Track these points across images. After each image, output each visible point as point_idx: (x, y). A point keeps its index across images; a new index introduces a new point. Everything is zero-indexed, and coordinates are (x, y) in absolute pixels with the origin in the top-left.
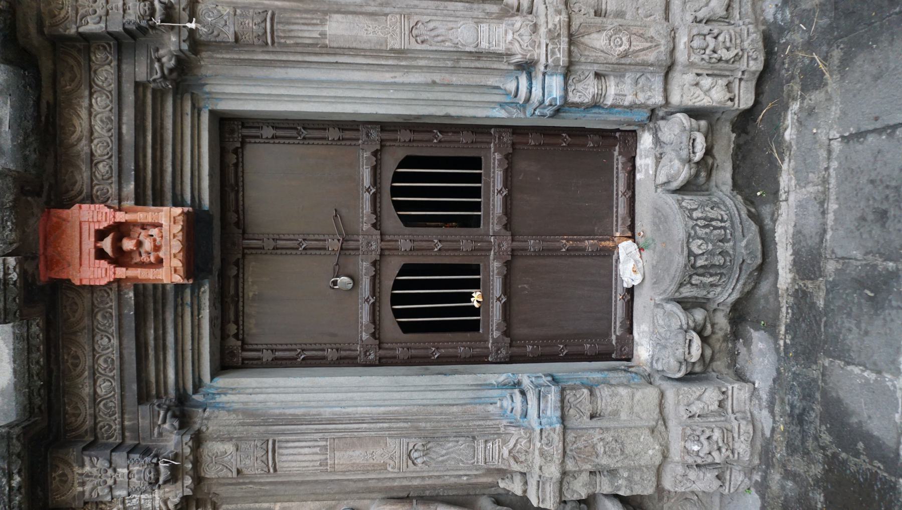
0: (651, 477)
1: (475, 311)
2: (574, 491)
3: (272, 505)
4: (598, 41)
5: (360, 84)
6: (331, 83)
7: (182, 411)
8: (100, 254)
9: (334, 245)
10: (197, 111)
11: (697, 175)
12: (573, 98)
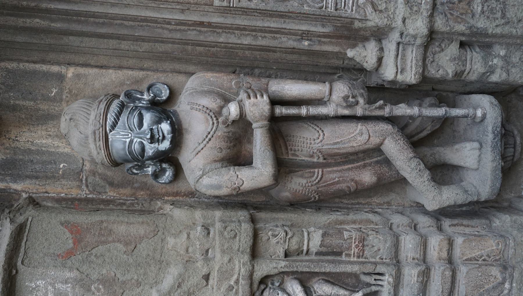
2: (439, 67)
3: (63, 69)
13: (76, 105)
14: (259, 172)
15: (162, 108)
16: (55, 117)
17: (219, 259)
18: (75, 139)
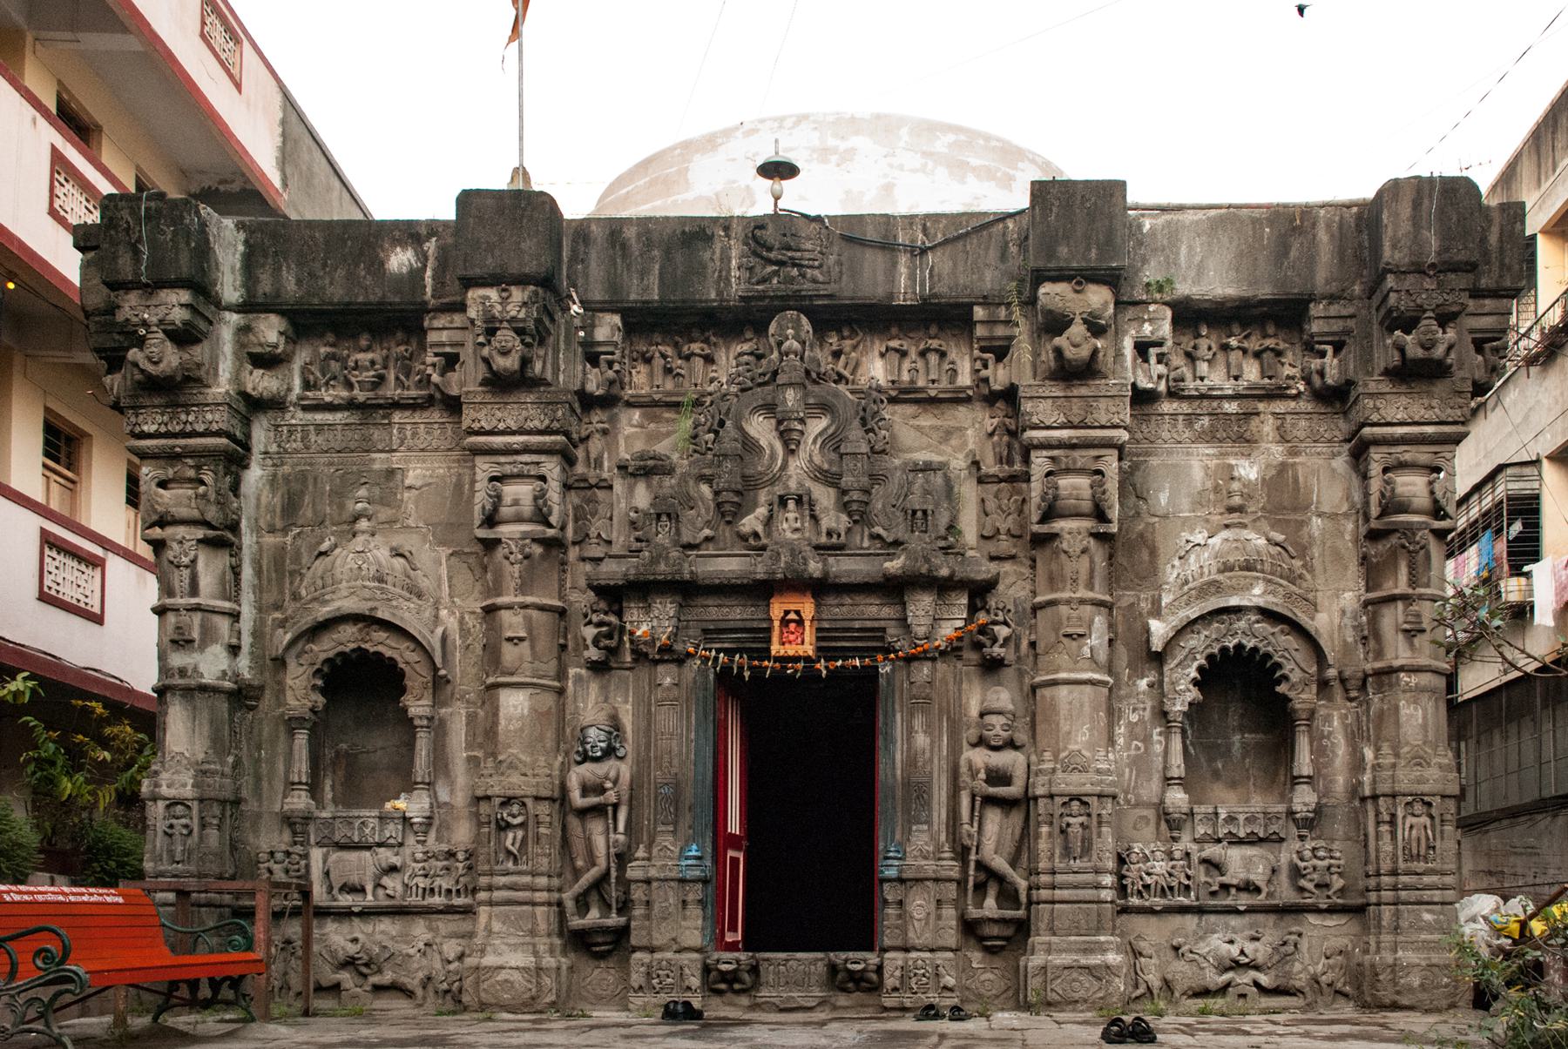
0: (644, 942)
8: (787, 612)
14: (577, 799)
15: (610, 752)
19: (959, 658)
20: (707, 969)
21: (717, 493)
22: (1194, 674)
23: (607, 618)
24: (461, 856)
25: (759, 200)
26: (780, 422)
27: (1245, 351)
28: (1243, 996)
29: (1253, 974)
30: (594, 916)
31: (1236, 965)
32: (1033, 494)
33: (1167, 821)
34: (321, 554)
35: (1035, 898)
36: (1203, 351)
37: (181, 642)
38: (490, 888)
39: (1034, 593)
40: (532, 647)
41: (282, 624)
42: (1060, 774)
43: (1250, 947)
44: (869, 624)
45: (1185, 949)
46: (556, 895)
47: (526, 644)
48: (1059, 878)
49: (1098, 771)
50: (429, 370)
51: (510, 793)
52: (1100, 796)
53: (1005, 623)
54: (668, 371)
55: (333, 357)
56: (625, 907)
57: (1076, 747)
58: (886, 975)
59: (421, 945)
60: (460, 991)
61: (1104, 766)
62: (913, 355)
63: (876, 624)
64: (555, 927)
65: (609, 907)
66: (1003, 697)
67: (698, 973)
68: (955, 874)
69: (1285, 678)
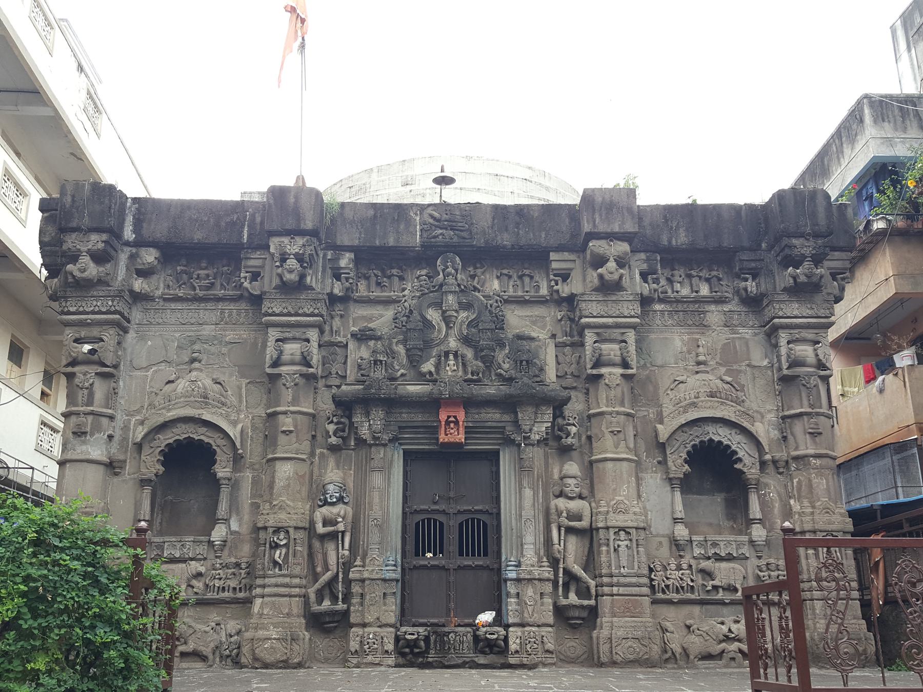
1: (424, 555)
4: (530, 592)
5: (510, 502)
6: (510, 491)
7: (393, 440)
8: (449, 417)
9: (452, 494)
10: (499, 444)
11: (482, 640)
12: (509, 583)
13: (342, 475)
14: (320, 529)
15: (341, 499)
16: (338, 469)
17: (295, 517)
18: (331, 474)
19: (547, 445)
20: (397, 639)
21: (407, 350)
22: (684, 455)
23: (342, 420)
24: (243, 566)
25: (430, 195)
26: (444, 312)
27: (700, 277)
28: (733, 659)
29: (737, 644)
30: (326, 604)
31: (727, 639)
32: (587, 353)
33: (677, 545)
34: (169, 382)
35: (600, 593)
36: (677, 278)
37: (79, 434)
38: (264, 586)
39: (589, 409)
40: (297, 436)
41: (142, 423)
42: (611, 514)
43: (734, 627)
44: (494, 424)
45: (695, 626)
46: (304, 590)
47: (294, 434)
48: (615, 579)
49: (635, 514)
50: (243, 280)
51: (280, 525)
52: (637, 528)
53: (574, 425)
54: (378, 284)
55: (183, 272)
56: (347, 598)
57: (622, 498)
58: (511, 643)
59: (213, 624)
60: (237, 655)
61: (637, 510)
62: (515, 277)
63: (500, 425)
64: (302, 612)
65: (338, 598)
66: (572, 468)
67: (392, 641)
68: (552, 577)
69: (740, 460)
